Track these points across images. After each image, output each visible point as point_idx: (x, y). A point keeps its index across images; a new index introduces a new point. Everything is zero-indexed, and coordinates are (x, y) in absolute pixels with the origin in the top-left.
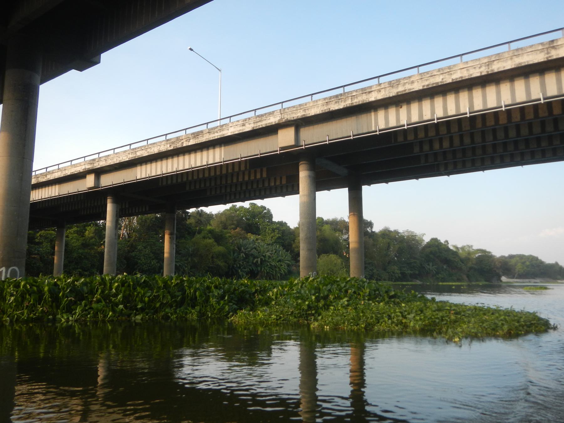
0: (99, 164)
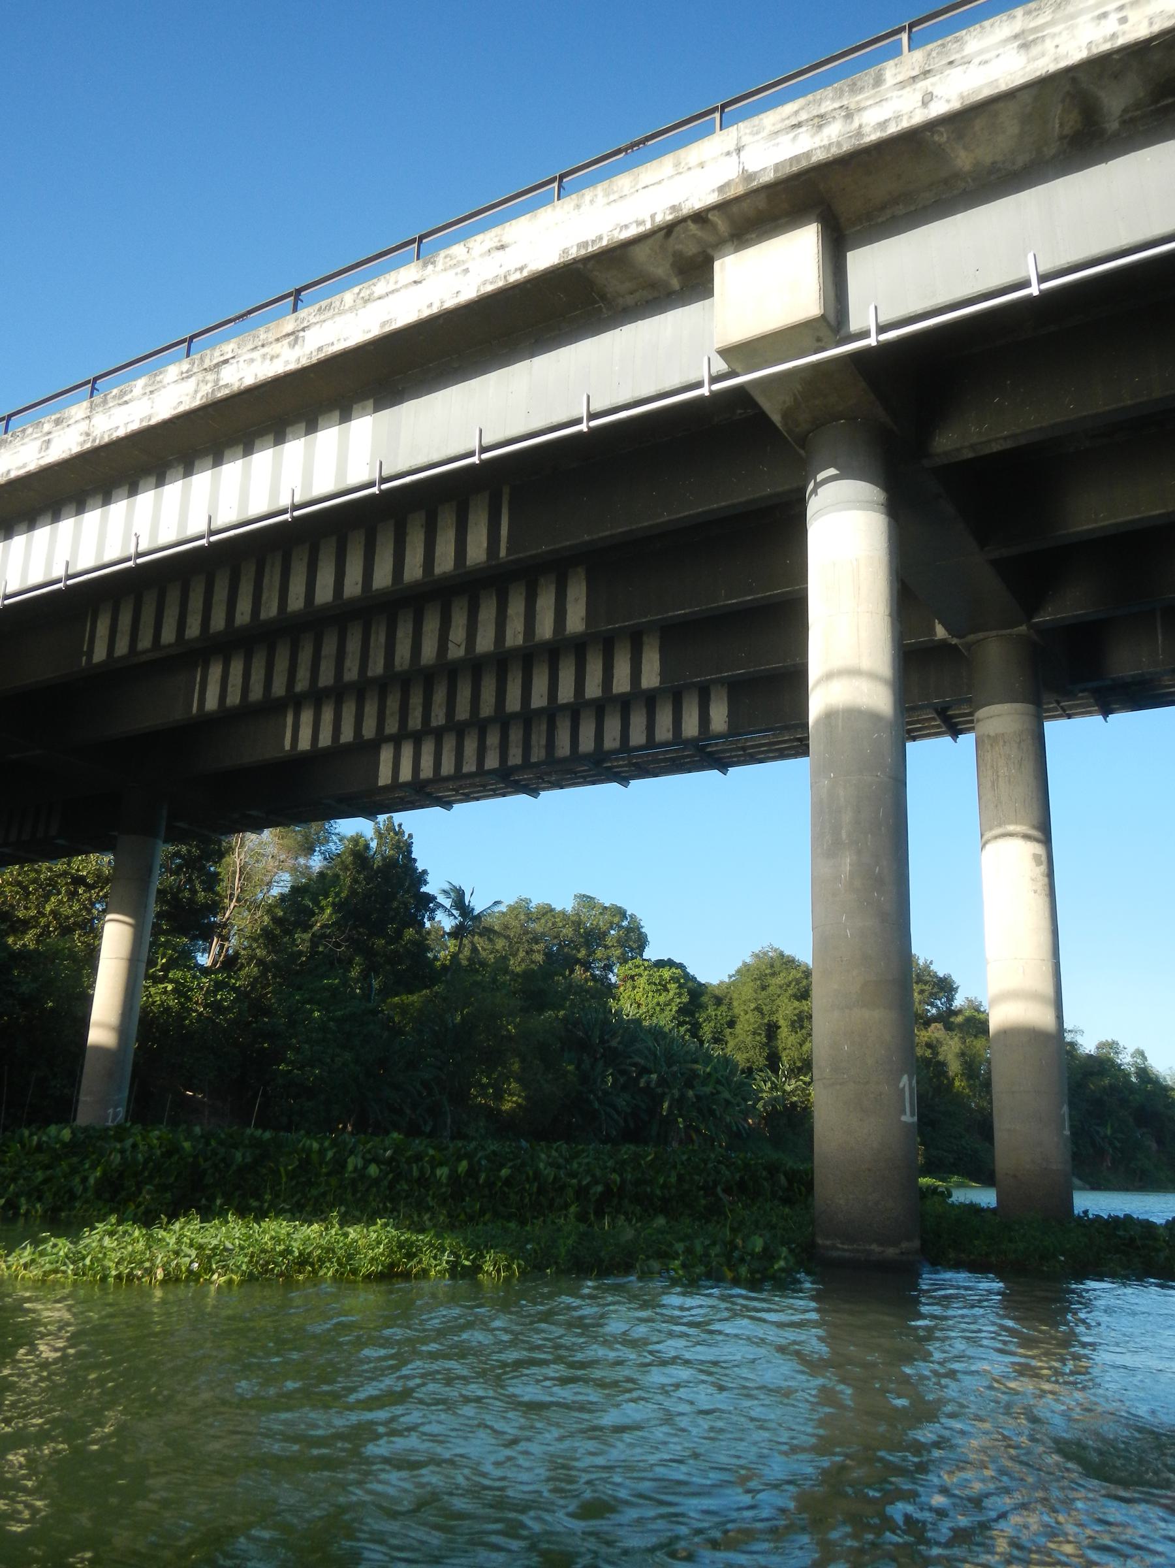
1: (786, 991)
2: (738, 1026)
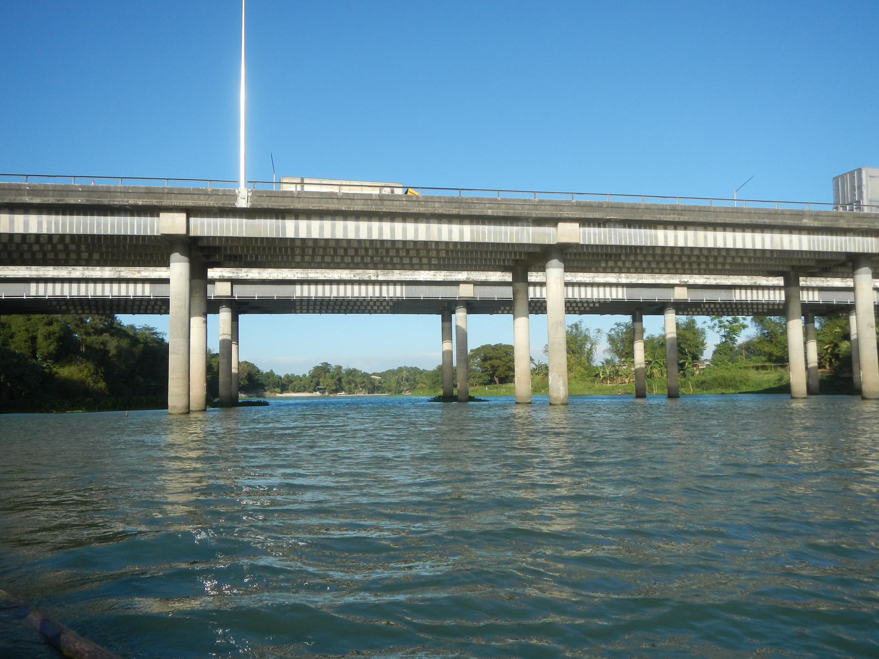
0: (247, 276)
1: (42, 321)
2: (16, 339)
